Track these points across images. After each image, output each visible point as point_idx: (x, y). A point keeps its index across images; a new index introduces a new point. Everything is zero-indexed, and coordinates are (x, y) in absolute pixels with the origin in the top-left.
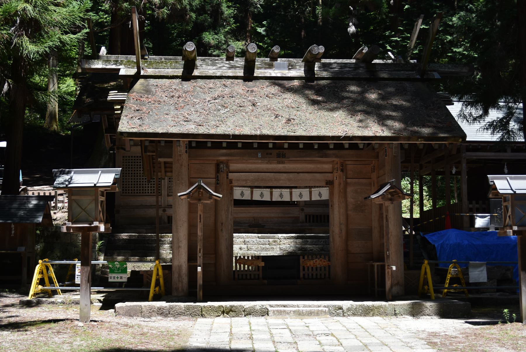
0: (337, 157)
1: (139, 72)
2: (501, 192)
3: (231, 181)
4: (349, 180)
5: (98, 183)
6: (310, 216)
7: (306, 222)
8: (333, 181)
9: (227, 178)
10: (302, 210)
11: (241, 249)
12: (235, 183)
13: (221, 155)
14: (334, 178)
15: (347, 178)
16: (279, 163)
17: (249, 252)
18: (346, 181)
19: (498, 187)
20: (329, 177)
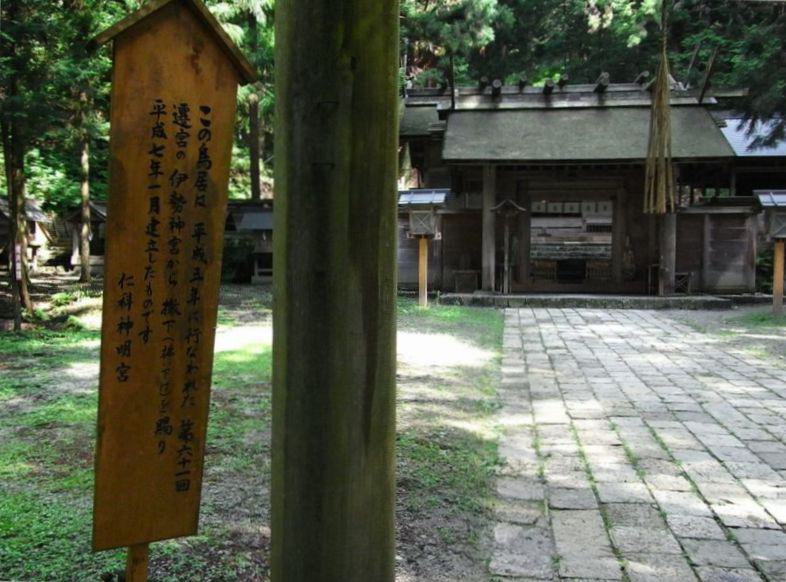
2: (765, 204)
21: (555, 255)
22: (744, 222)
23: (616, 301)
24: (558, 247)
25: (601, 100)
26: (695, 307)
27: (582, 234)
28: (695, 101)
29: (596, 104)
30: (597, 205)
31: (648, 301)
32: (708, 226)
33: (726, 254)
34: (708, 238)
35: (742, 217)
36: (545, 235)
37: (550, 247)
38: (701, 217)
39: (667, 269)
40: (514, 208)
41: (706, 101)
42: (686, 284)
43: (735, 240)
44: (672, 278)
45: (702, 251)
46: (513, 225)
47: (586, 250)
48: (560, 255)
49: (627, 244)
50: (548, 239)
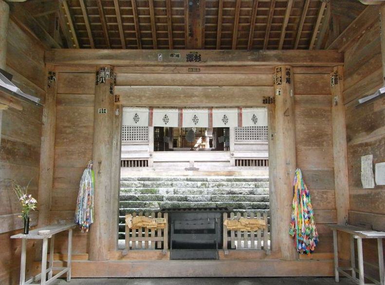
3: (117, 99)
4: (298, 97)
6: (239, 160)
7: (236, 165)
9: (111, 92)
10: (233, 155)
11: (167, 192)
12: (122, 101)
14: (275, 93)
15: (295, 93)
16: (192, 70)
17: (175, 195)
18: (294, 98)
20: (268, 92)
24: (199, 184)
27: (230, 168)
30: (240, 115)
37: (189, 183)
48: (201, 192)
49: (299, 185)
50: (195, 173)
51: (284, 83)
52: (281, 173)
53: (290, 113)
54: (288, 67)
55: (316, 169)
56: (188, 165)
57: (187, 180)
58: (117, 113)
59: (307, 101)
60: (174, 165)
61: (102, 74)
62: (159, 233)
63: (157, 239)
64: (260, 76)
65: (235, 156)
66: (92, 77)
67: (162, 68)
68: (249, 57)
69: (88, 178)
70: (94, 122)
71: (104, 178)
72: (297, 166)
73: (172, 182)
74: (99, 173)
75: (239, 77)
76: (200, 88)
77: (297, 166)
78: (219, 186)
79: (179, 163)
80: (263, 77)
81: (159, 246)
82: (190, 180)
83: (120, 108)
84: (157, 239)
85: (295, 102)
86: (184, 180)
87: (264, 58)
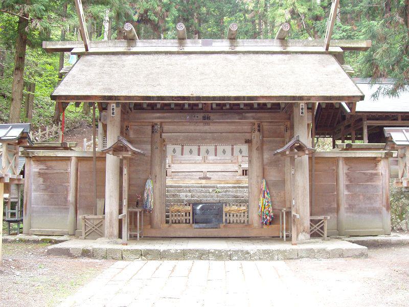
0: (254, 118)
1: (87, 50)
2: (398, 143)
3: (164, 141)
5: (4, 136)
8: (251, 140)
9: (161, 137)
10: (240, 166)
11: (186, 196)
13: (155, 117)
14: (252, 136)
15: (263, 137)
16: (206, 124)
18: (263, 139)
19: (394, 139)
20: (248, 136)
21: (207, 197)
22: (376, 166)
23: (242, 251)
24: (211, 190)
25: (232, 45)
26: (331, 255)
27: (238, 177)
28: (323, 49)
29: (227, 49)
31: (278, 250)
32: (342, 169)
33: (361, 197)
34: (343, 181)
35: (375, 160)
36: (205, 178)
38: (335, 160)
39: (298, 216)
40: (126, 149)
41: (331, 49)
42: (322, 228)
43: (369, 183)
44: (307, 223)
45: (338, 195)
46: (140, 168)
47: (236, 192)
48: (212, 197)
50: (208, 181)
51: (256, 132)
52: (254, 181)
53: (261, 149)
54: (259, 123)
55: (275, 179)
56: (202, 175)
57: (201, 187)
58: (164, 149)
59: (270, 142)
60: (190, 175)
61: (156, 127)
62: (188, 214)
63: (186, 218)
64: (243, 127)
65: (242, 167)
66: (150, 128)
67: (189, 123)
68: (237, 117)
69: (149, 185)
70: (151, 154)
71: (158, 185)
72: (264, 178)
73: (189, 189)
74: (155, 182)
75: (232, 127)
76: (211, 134)
77: (264, 178)
78: (226, 191)
79: (193, 173)
80: (246, 127)
81: (188, 221)
82: (204, 187)
83: (165, 145)
84: (186, 218)
85: (262, 143)
86: (198, 187)
87: (245, 118)
